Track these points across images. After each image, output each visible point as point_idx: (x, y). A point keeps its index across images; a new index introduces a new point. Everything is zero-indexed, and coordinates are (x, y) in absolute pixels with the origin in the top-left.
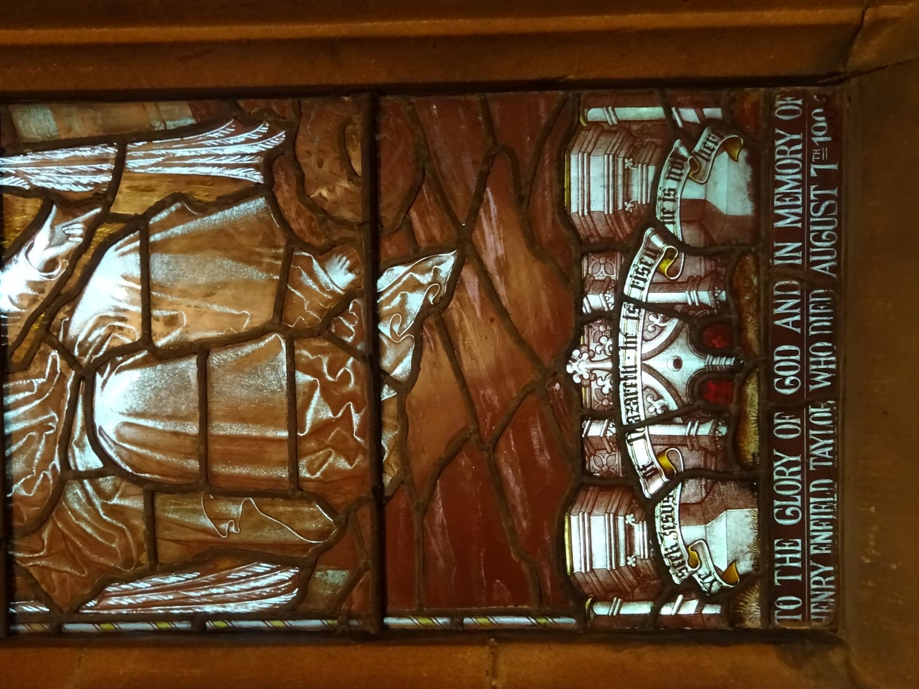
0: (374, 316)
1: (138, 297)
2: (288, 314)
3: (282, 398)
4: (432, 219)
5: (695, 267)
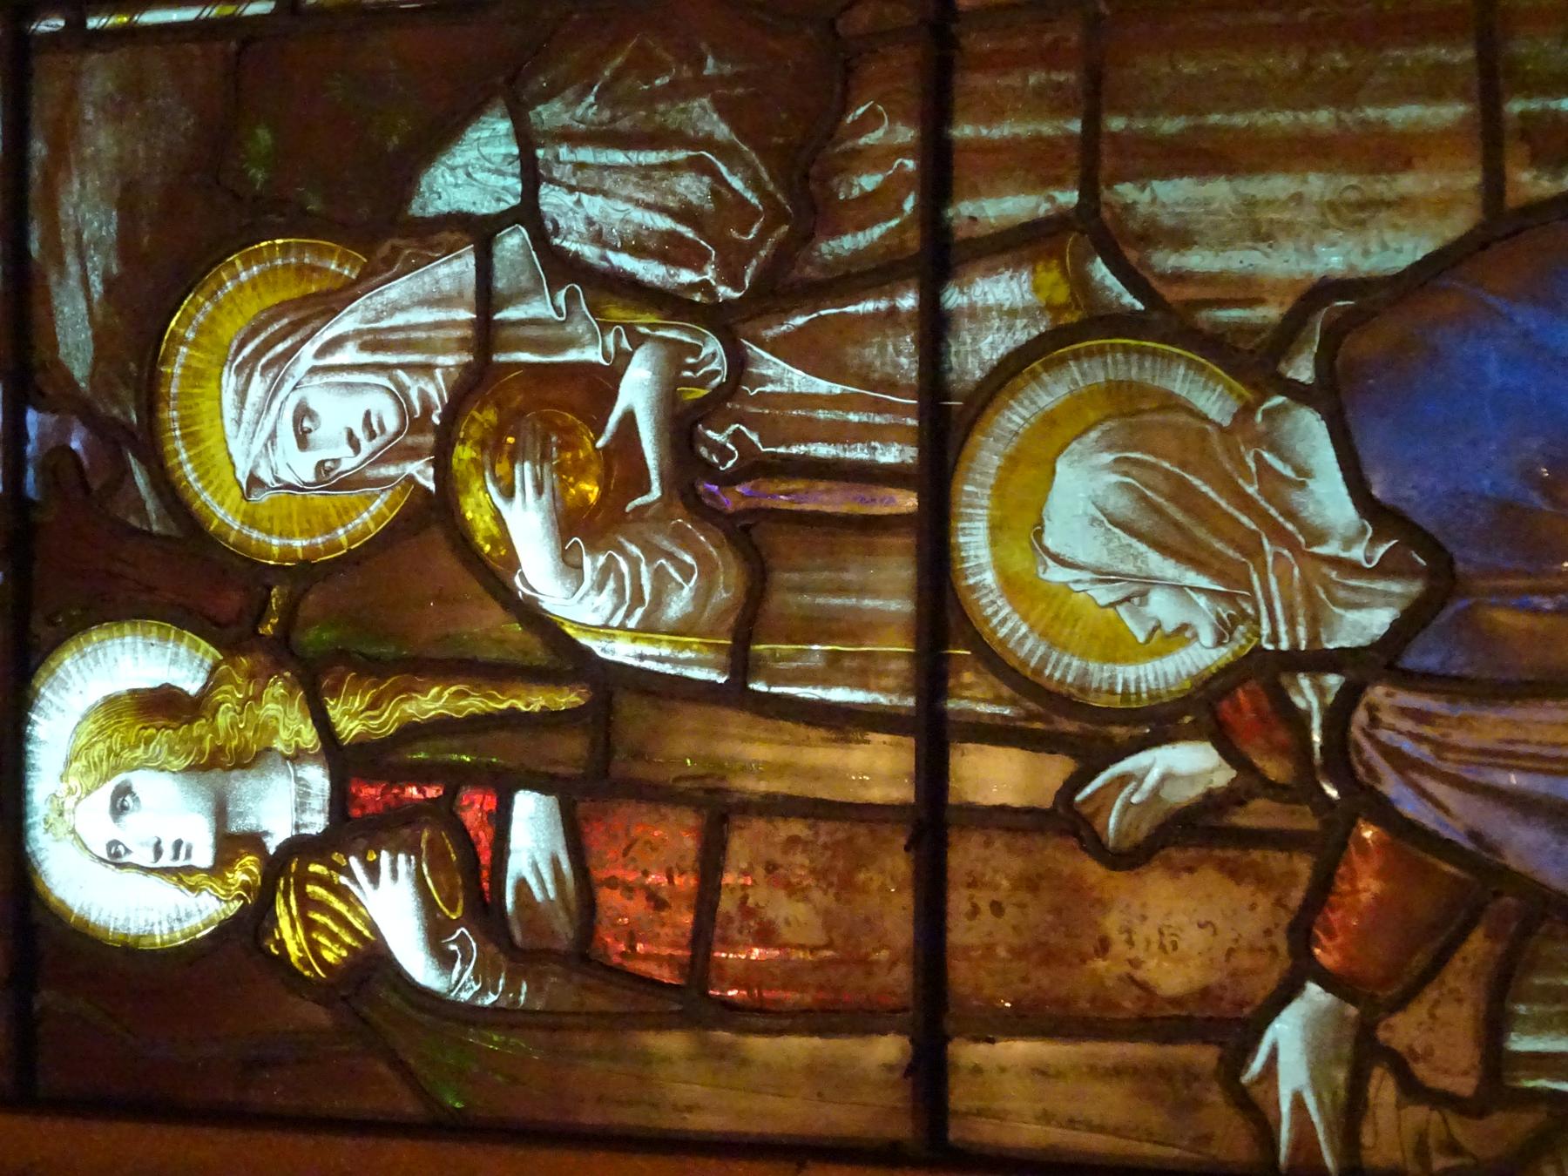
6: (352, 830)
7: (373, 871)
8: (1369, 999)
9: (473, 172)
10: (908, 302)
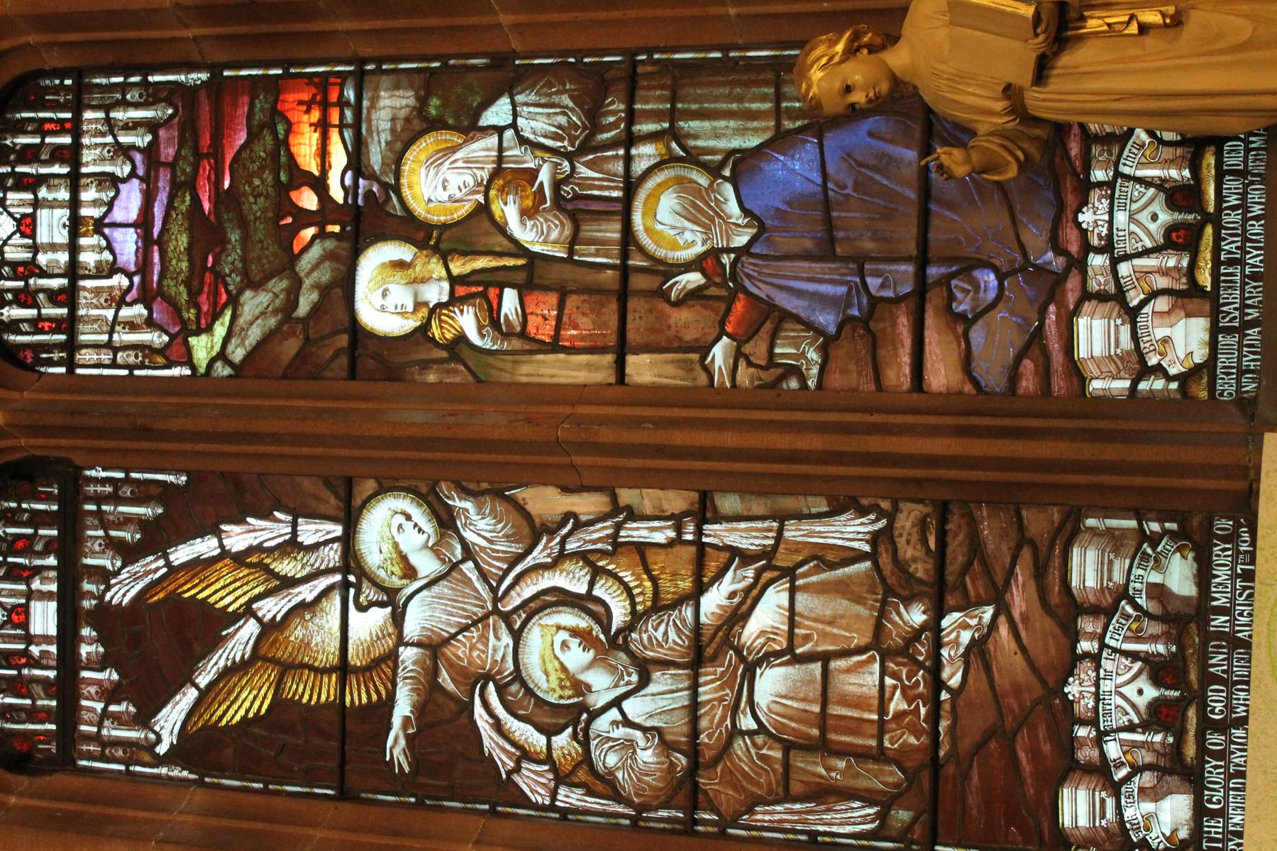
0: (938, 644)
1: (786, 621)
2: (882, 638)
3: (874, 692)
4: (980, 583)
5: (1155, 628)
6: (454, 300)
7: (462, 312)
8: (740, 341)
9: (499, 113)
10: (621, 152)
